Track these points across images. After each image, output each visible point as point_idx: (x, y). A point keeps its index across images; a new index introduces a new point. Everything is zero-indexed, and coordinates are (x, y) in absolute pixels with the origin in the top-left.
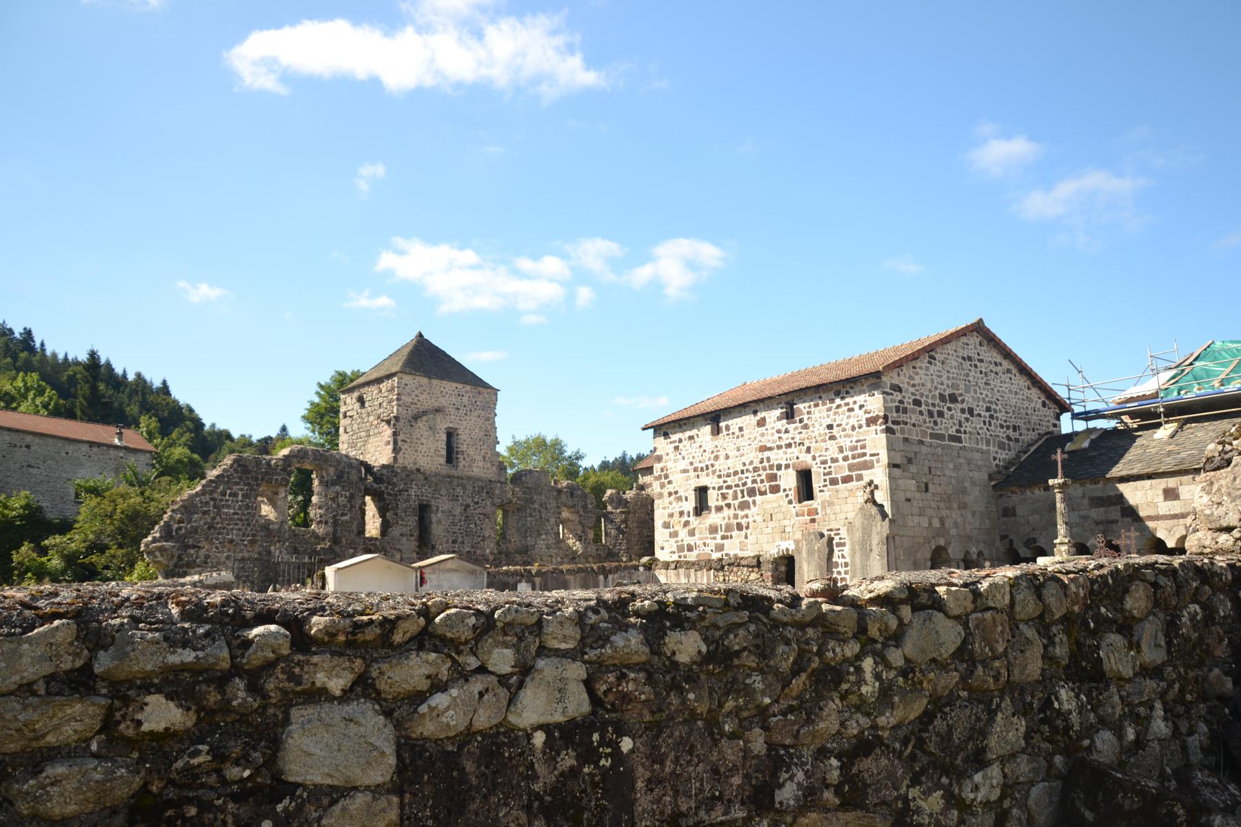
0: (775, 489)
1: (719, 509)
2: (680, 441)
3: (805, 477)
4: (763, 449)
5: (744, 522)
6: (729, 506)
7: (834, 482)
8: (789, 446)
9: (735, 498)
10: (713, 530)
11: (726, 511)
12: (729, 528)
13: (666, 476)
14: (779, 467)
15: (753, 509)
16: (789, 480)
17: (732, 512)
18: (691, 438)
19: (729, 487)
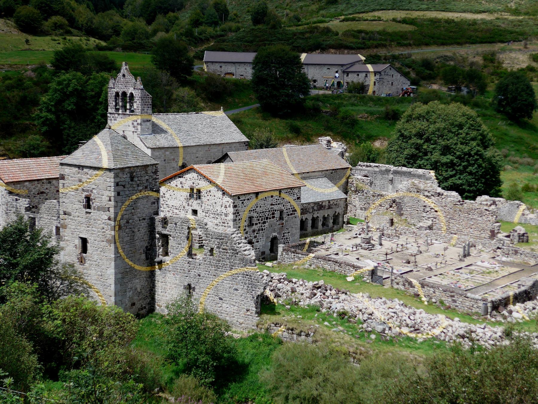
0: (273, 217)
1: (256, 224)
2: (244, 200)
3: (281, 212)
4: (272, 205)
5: (264, 228)
6: (259, 223)
7: (288, 215)
8: (279, 204)
9: (262, 220)
10: (254, 231)
11: (259, 225)
12: (259, 230)
13: (238, 213)
14: (276, 210)
15: (267, 224)
16: (277, 215)
17: (260, 225)
18: (248, 199)
19: (260, 217)
